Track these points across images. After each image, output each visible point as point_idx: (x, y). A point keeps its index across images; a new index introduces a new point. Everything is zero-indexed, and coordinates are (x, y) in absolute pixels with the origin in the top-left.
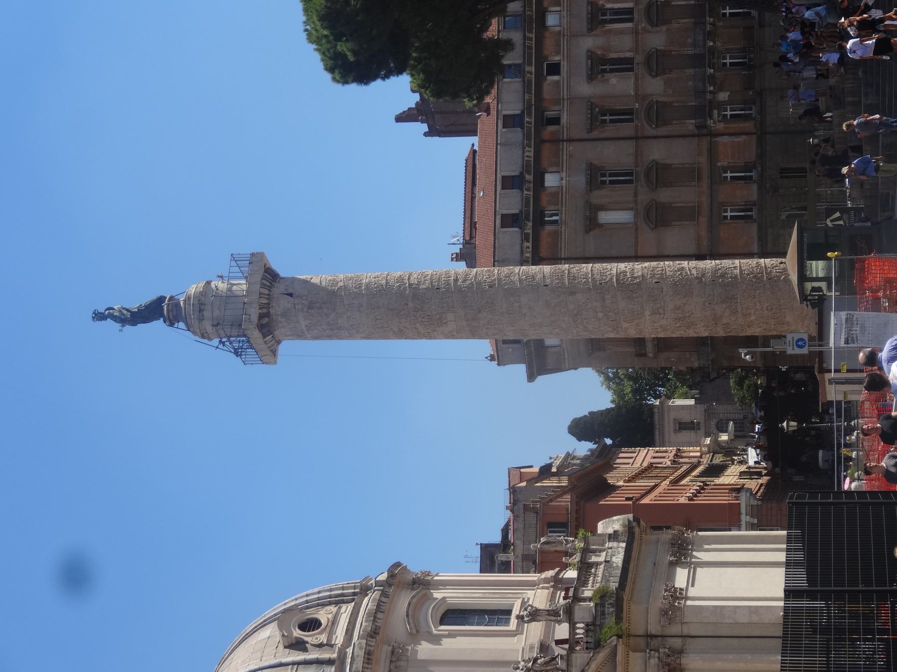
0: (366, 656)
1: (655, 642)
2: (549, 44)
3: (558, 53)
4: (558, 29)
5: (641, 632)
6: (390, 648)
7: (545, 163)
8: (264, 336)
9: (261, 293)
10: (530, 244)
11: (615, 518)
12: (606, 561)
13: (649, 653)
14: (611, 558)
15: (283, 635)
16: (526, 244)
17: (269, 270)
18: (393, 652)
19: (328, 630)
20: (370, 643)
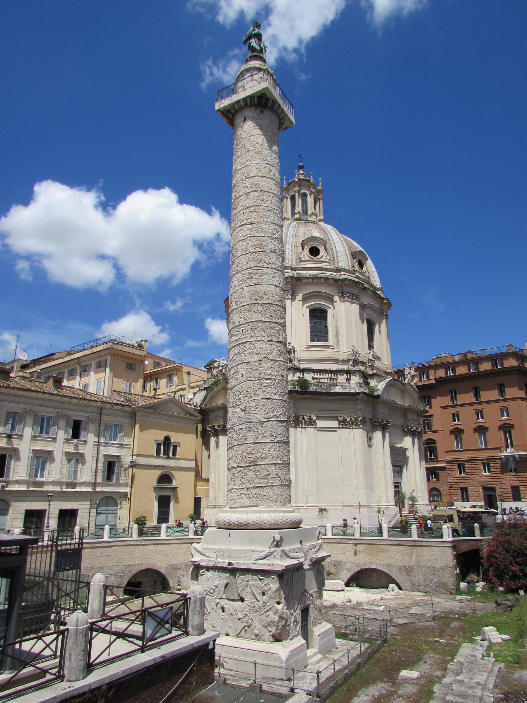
6: (290, 289)
12: (337, 384)
14: (340, 386)
15: (303, 241)
17: (264, 100)
19: (312, 260)
20: (288, 278)
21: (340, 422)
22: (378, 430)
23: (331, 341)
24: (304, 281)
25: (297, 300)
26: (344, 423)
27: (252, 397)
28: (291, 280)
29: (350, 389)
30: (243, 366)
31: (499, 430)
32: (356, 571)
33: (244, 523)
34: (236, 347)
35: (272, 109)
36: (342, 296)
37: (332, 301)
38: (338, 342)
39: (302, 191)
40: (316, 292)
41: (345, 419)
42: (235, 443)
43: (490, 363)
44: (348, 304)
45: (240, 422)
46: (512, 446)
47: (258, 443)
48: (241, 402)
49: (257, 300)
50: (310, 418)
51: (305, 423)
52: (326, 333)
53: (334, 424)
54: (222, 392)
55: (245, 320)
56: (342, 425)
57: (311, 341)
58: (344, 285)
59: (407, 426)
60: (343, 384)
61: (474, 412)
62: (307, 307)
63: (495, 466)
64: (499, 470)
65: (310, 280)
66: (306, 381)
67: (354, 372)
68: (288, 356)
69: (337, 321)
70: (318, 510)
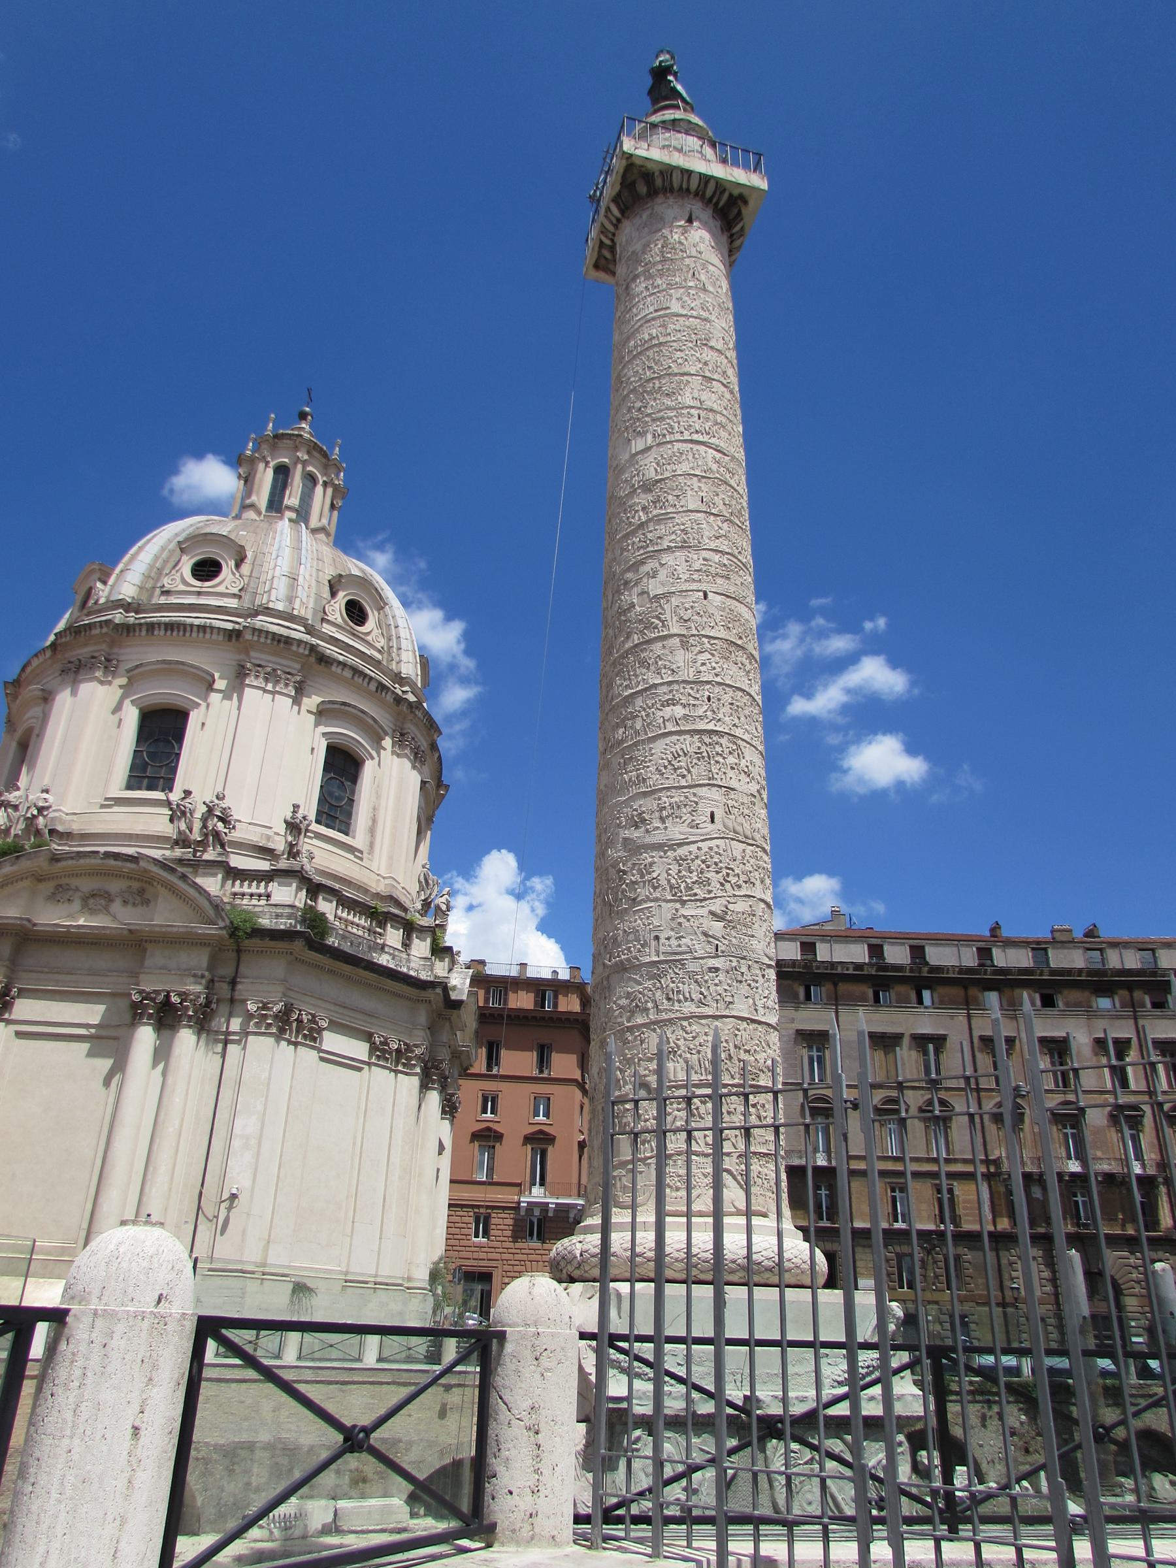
0: (283, 639)
1: (223, 989)
2: (1076, 995)
3: (1067, 1004)
4: (1094, 1005)
5: (242, 969)
7: (942, 990)
8: (616, 200)
9: (689, 173)
10: (851, 972)
11: (468, 981)
13: (203, 976)
14: (390, 954)
15: (340, 576)
16: (851, 967)
18: (289, 673)
20: (303, 646)
21: (373, 1048)
22: (434, 1089)
23: (359, 839)
24: (334, 668)
25: (304, 708)
26: (384, 1051)
27: (739, 887)
28: (307, 652)
29: (409, 968)
30: (715, 794)
31: (524, 1144)
32: (437, 1467)
33: (766, 1263)
34: (688, 737)
35: (732, 242)
36: (401, 738)
37: (379, 748)
38: (372, 845)
39: (310, 468)
40: (355, 707)
41: (385, 1043)
42: (689, 1008)
43: (532, 996)
44: (407, 764)
45: (710, 949)
46: (542, 1184)
47: (760, 1023)
48: (710, 892)
49: (740, 638)
50: (313, 1020)
51: (298, 1032)
52: (349, 815)
53: (358, 1049)
54: (26, 883)
55: (717, 675)
56: (378, 1057)
57: (318, 822)
58: (411, 717)
59: (449, 1094)
60: (397, 953)
61: (480, 1095)
62: (324, 734)
63: (502, 1223)
64: (509, 1233)
65: (348, 674)
66: (322, 917)
67: (423, 930)
68: (290, 839)
69: (378, 797)
70: (291, 1286)
